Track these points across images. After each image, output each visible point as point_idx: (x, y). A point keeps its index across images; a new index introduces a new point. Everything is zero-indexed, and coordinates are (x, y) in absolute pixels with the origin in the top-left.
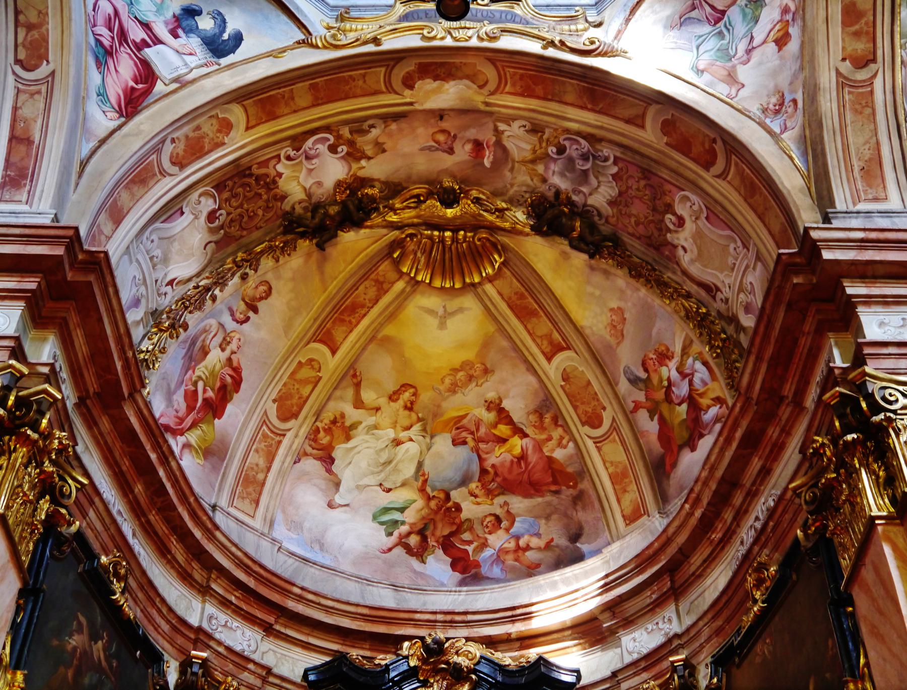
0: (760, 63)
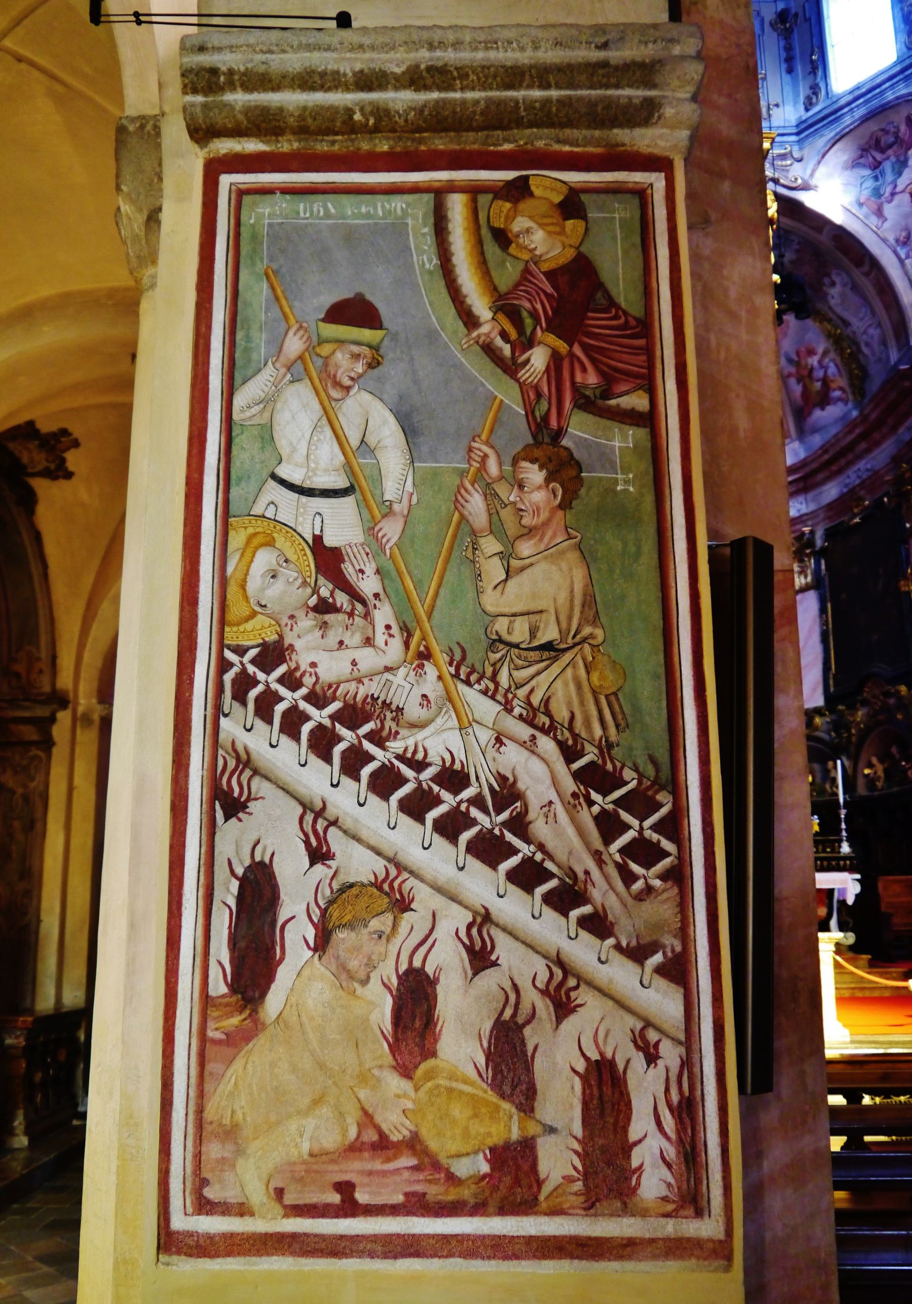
0: (899, 206)
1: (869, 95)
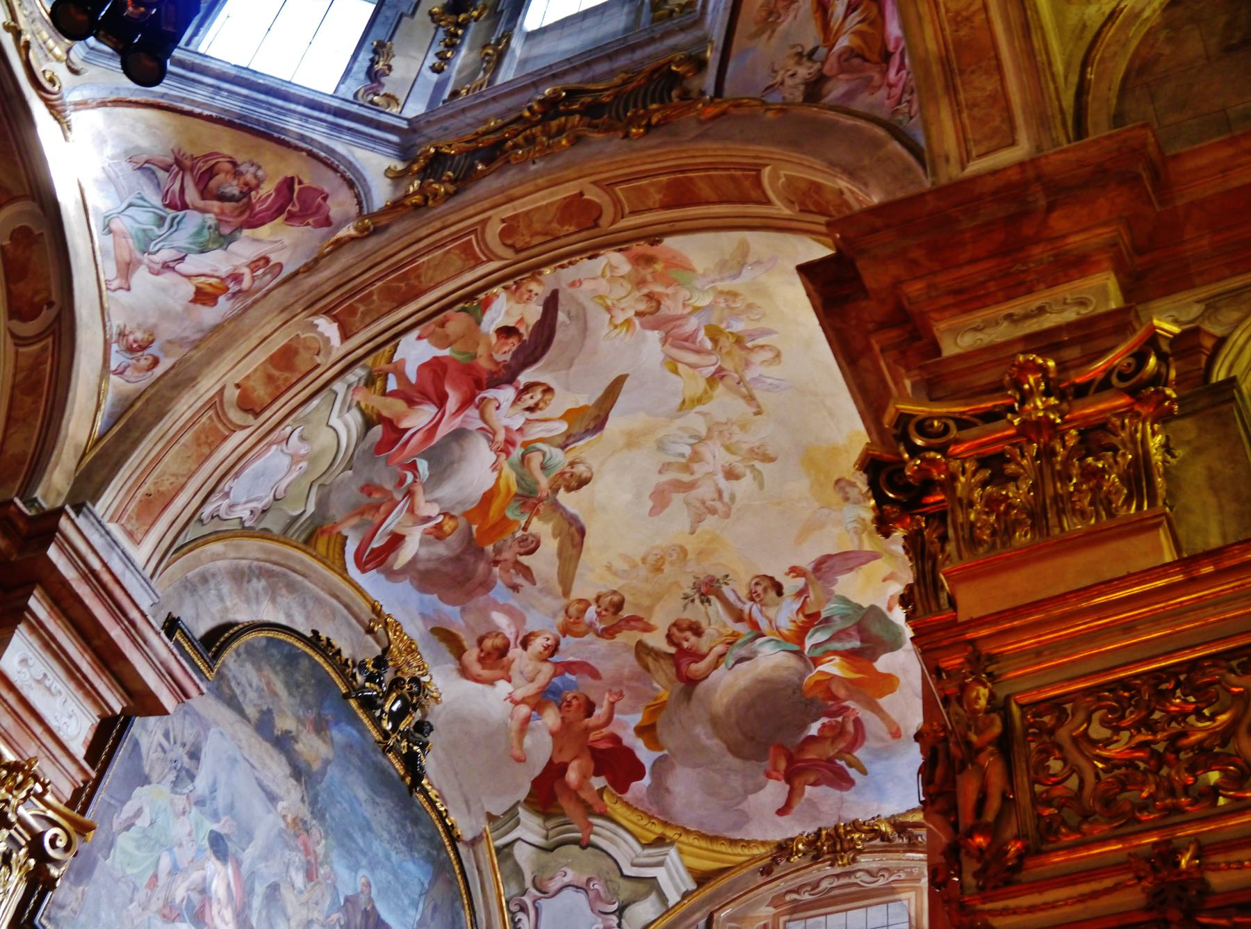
0: (164, 290)
1: (262, 97)
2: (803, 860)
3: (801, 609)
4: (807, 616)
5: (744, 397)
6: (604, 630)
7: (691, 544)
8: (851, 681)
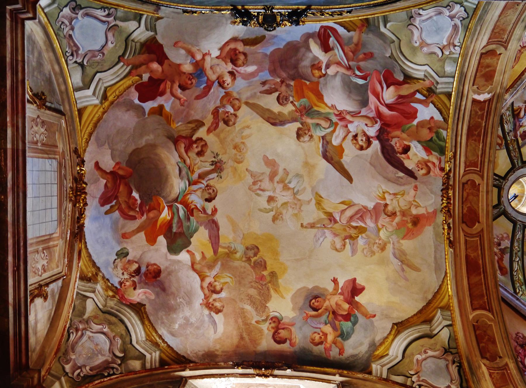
2: (76, 172)
3: (196, 208)
4: (193, 209)
5: (314, 223)
6: (218, 111)
7: (241, 167)
8: (157, 221)
